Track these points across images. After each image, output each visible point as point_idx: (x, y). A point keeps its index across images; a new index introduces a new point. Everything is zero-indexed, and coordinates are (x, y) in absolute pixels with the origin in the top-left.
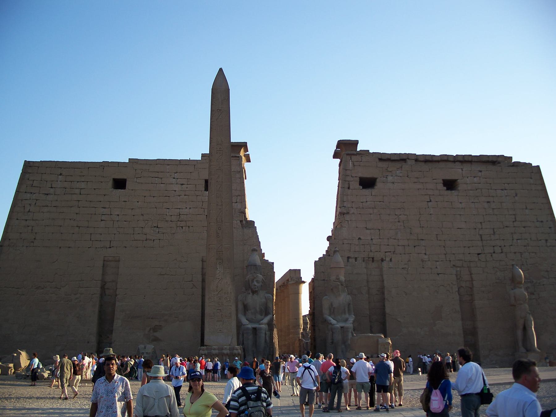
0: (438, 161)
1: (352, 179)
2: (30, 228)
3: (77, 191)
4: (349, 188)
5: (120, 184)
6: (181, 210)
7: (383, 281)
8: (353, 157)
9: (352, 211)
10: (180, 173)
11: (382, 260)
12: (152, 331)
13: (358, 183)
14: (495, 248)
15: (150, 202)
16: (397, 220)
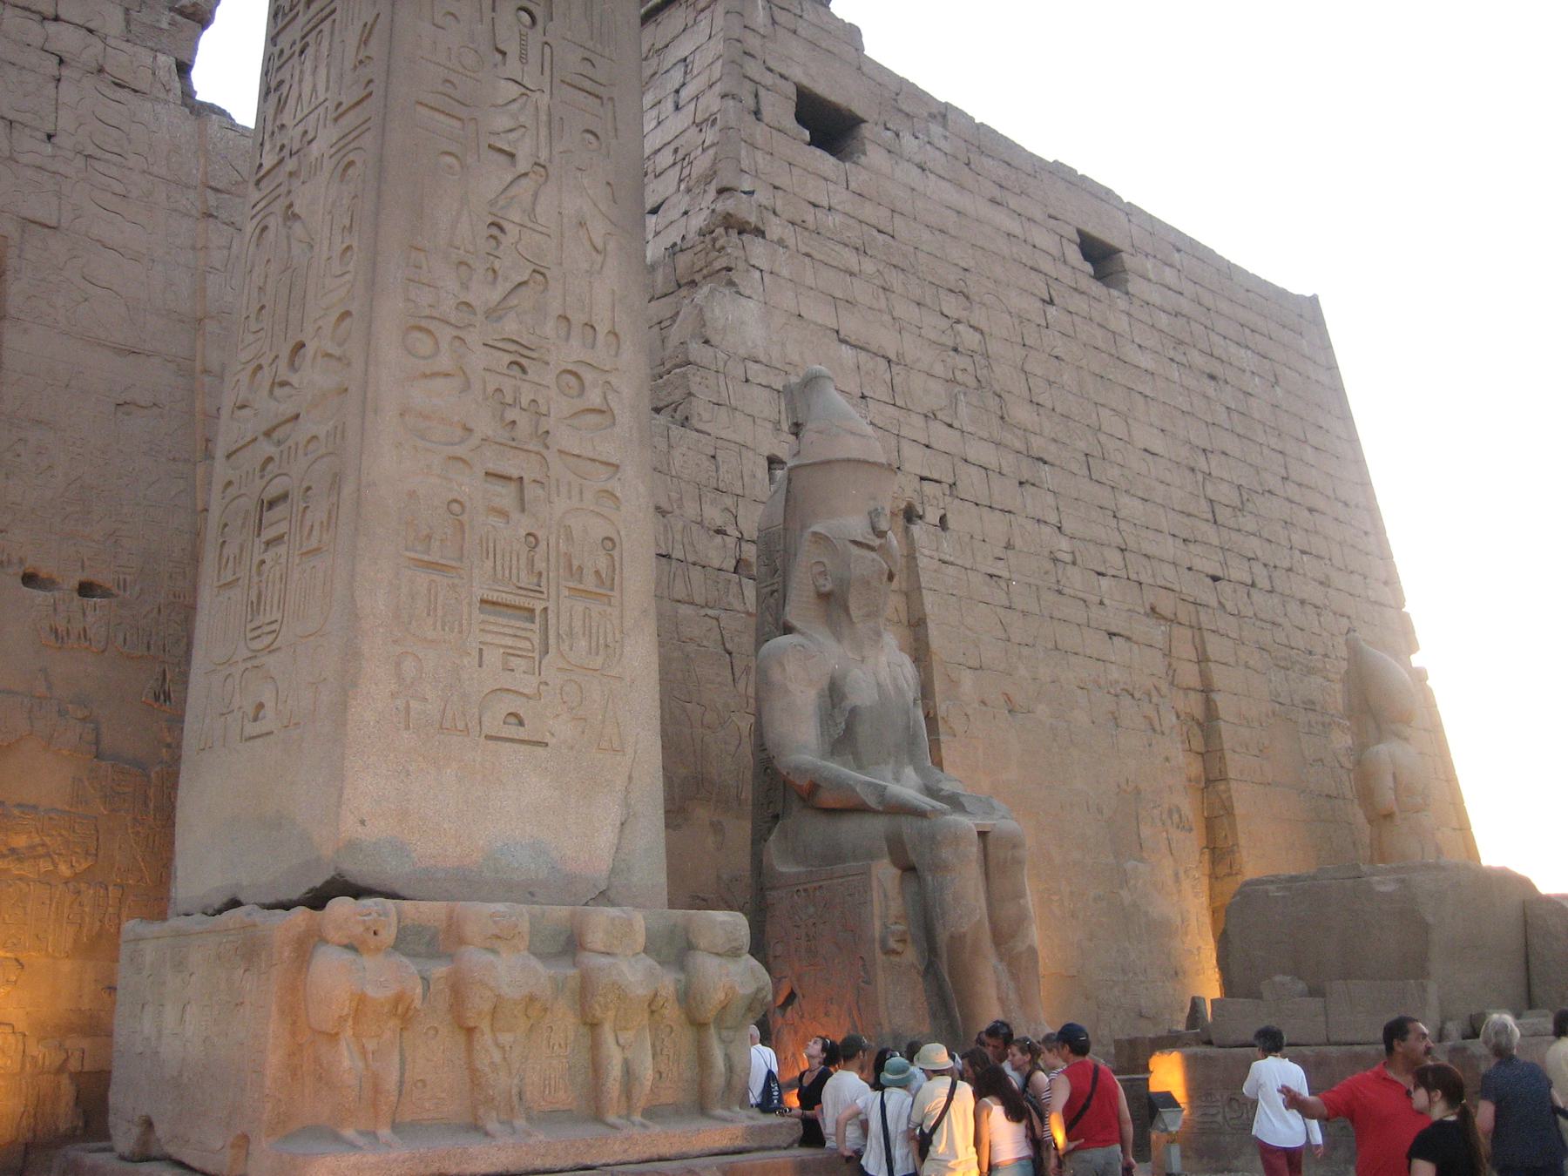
1: (769, 79)
4: (757, 113)
9: (775, 229)
11: (910, 515)
13: (791, 108)
16: (951, 343)
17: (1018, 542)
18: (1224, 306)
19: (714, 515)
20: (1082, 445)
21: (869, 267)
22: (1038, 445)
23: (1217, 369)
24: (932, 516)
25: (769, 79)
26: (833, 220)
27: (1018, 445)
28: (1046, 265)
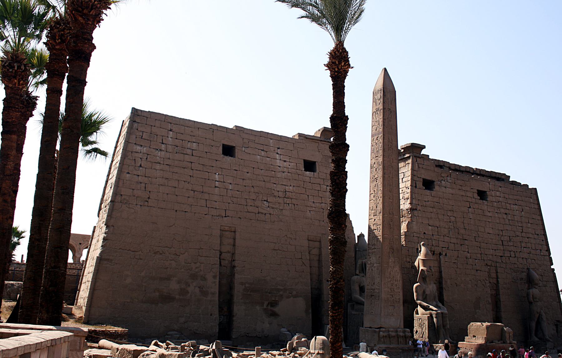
0: (462, 172)
1: (418, 179)
2: (143, 185)
3: (189, 152)
4: (416, 187)
5: (228, 151)
6: (287, 187)
7: (440, 272)
8: (418, 159)
9: (419, 208)
10: (282, 149)
11: (440, 254)
12: (269, 306)
13: (422, 183)
14: (511, 253)
15: (259, 175)
17: (460, 256)
18: (511, 197)
19: (408, 260)
20: (474, 235)
21: (435, 210)
22: (465, 237)
23: (507, 211)
24: (444, 254)
25: (418, 179)
26: (428, 203)
27: (461, 238)
28: (469, 199)
